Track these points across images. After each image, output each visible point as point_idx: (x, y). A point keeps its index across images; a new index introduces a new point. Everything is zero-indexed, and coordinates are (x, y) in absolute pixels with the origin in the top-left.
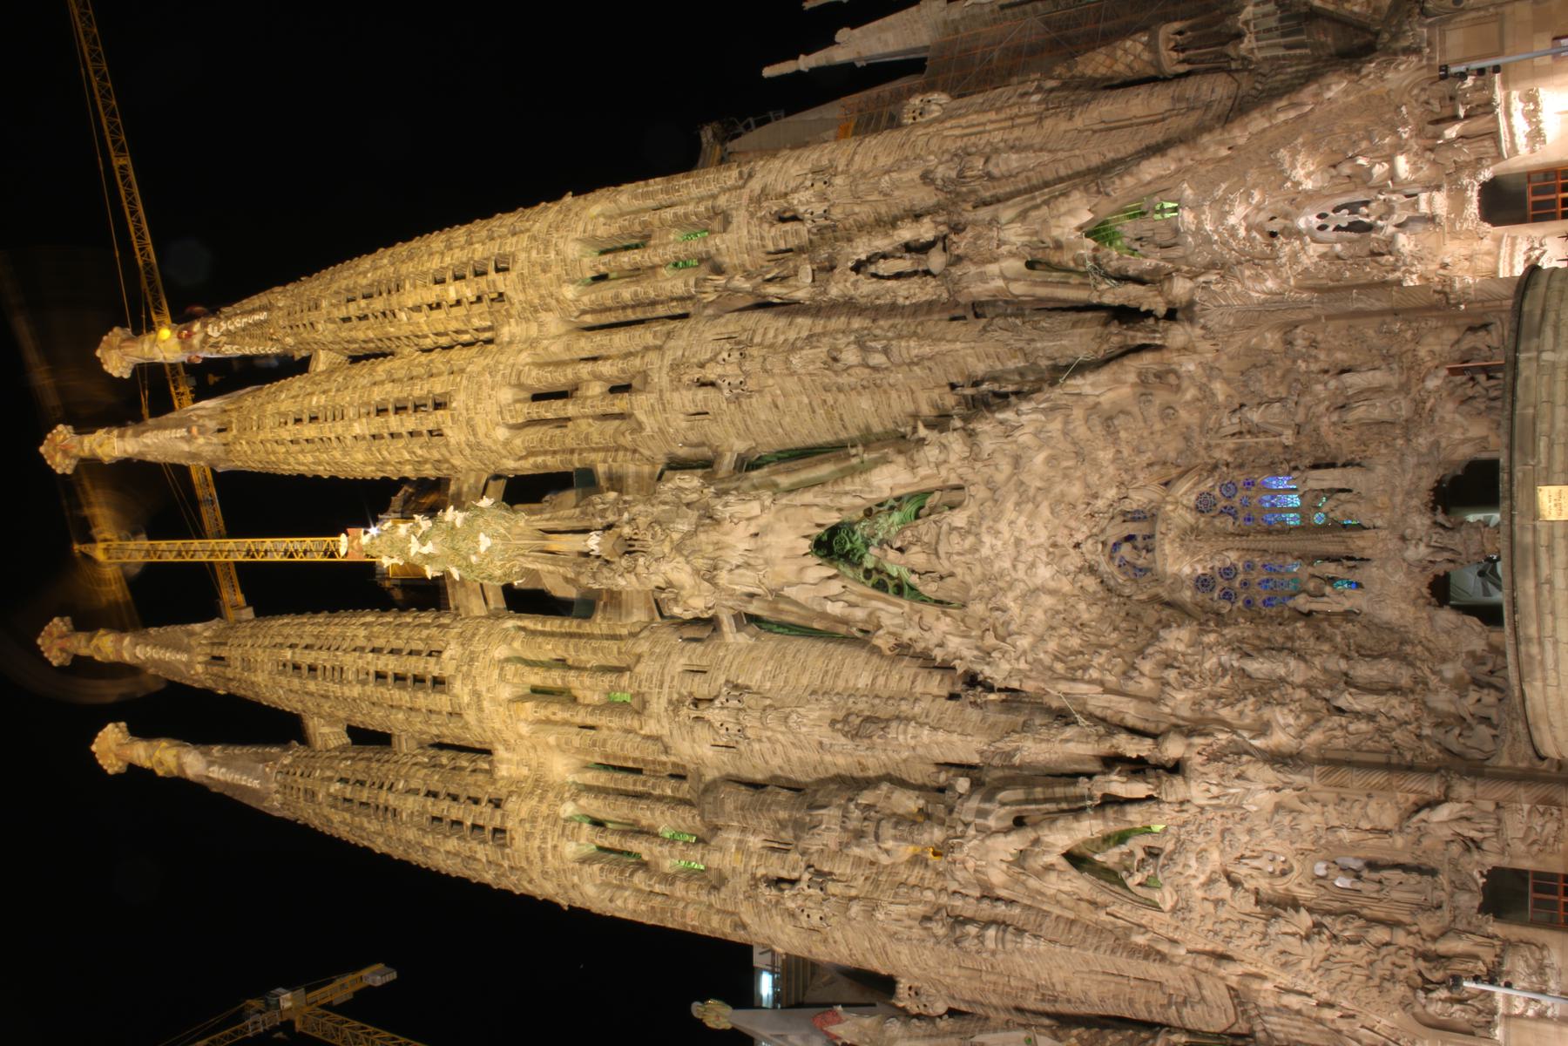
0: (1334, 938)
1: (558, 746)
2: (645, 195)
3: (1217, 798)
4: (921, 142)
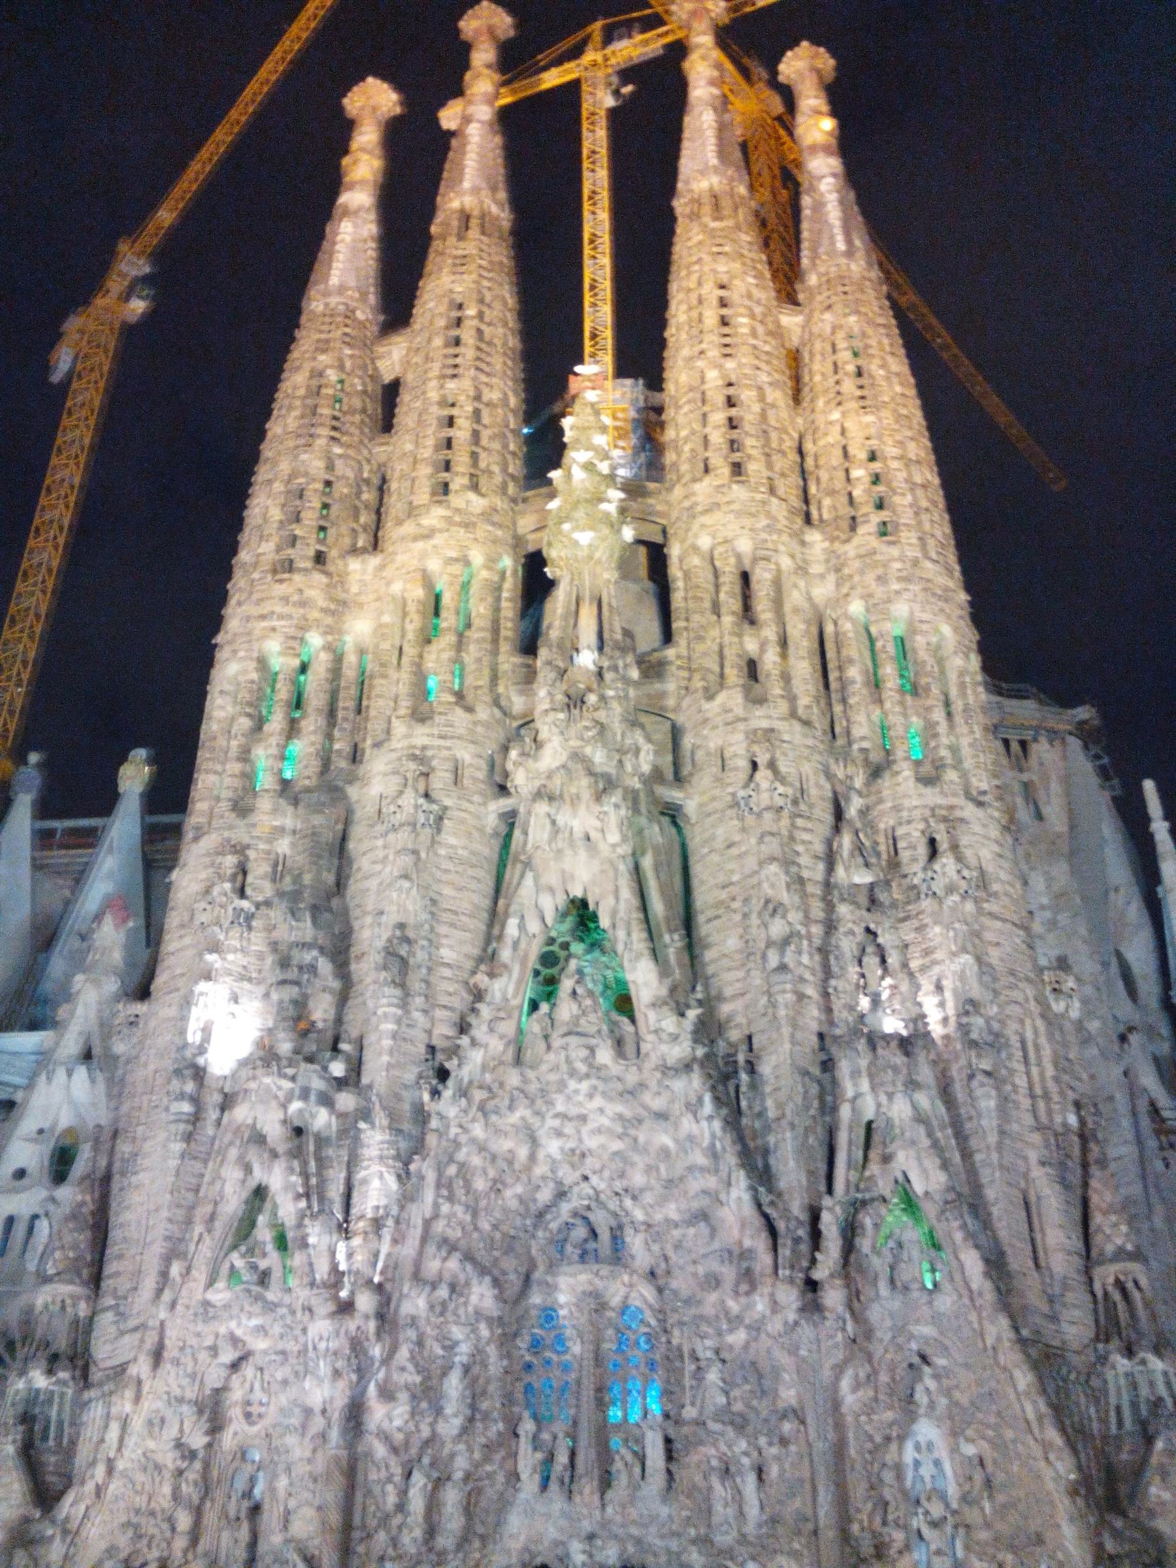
0: (180, 1473)
1: (381, 626)
2: (962, 686)
3: (315, 1348)
4: (1016, 995)
